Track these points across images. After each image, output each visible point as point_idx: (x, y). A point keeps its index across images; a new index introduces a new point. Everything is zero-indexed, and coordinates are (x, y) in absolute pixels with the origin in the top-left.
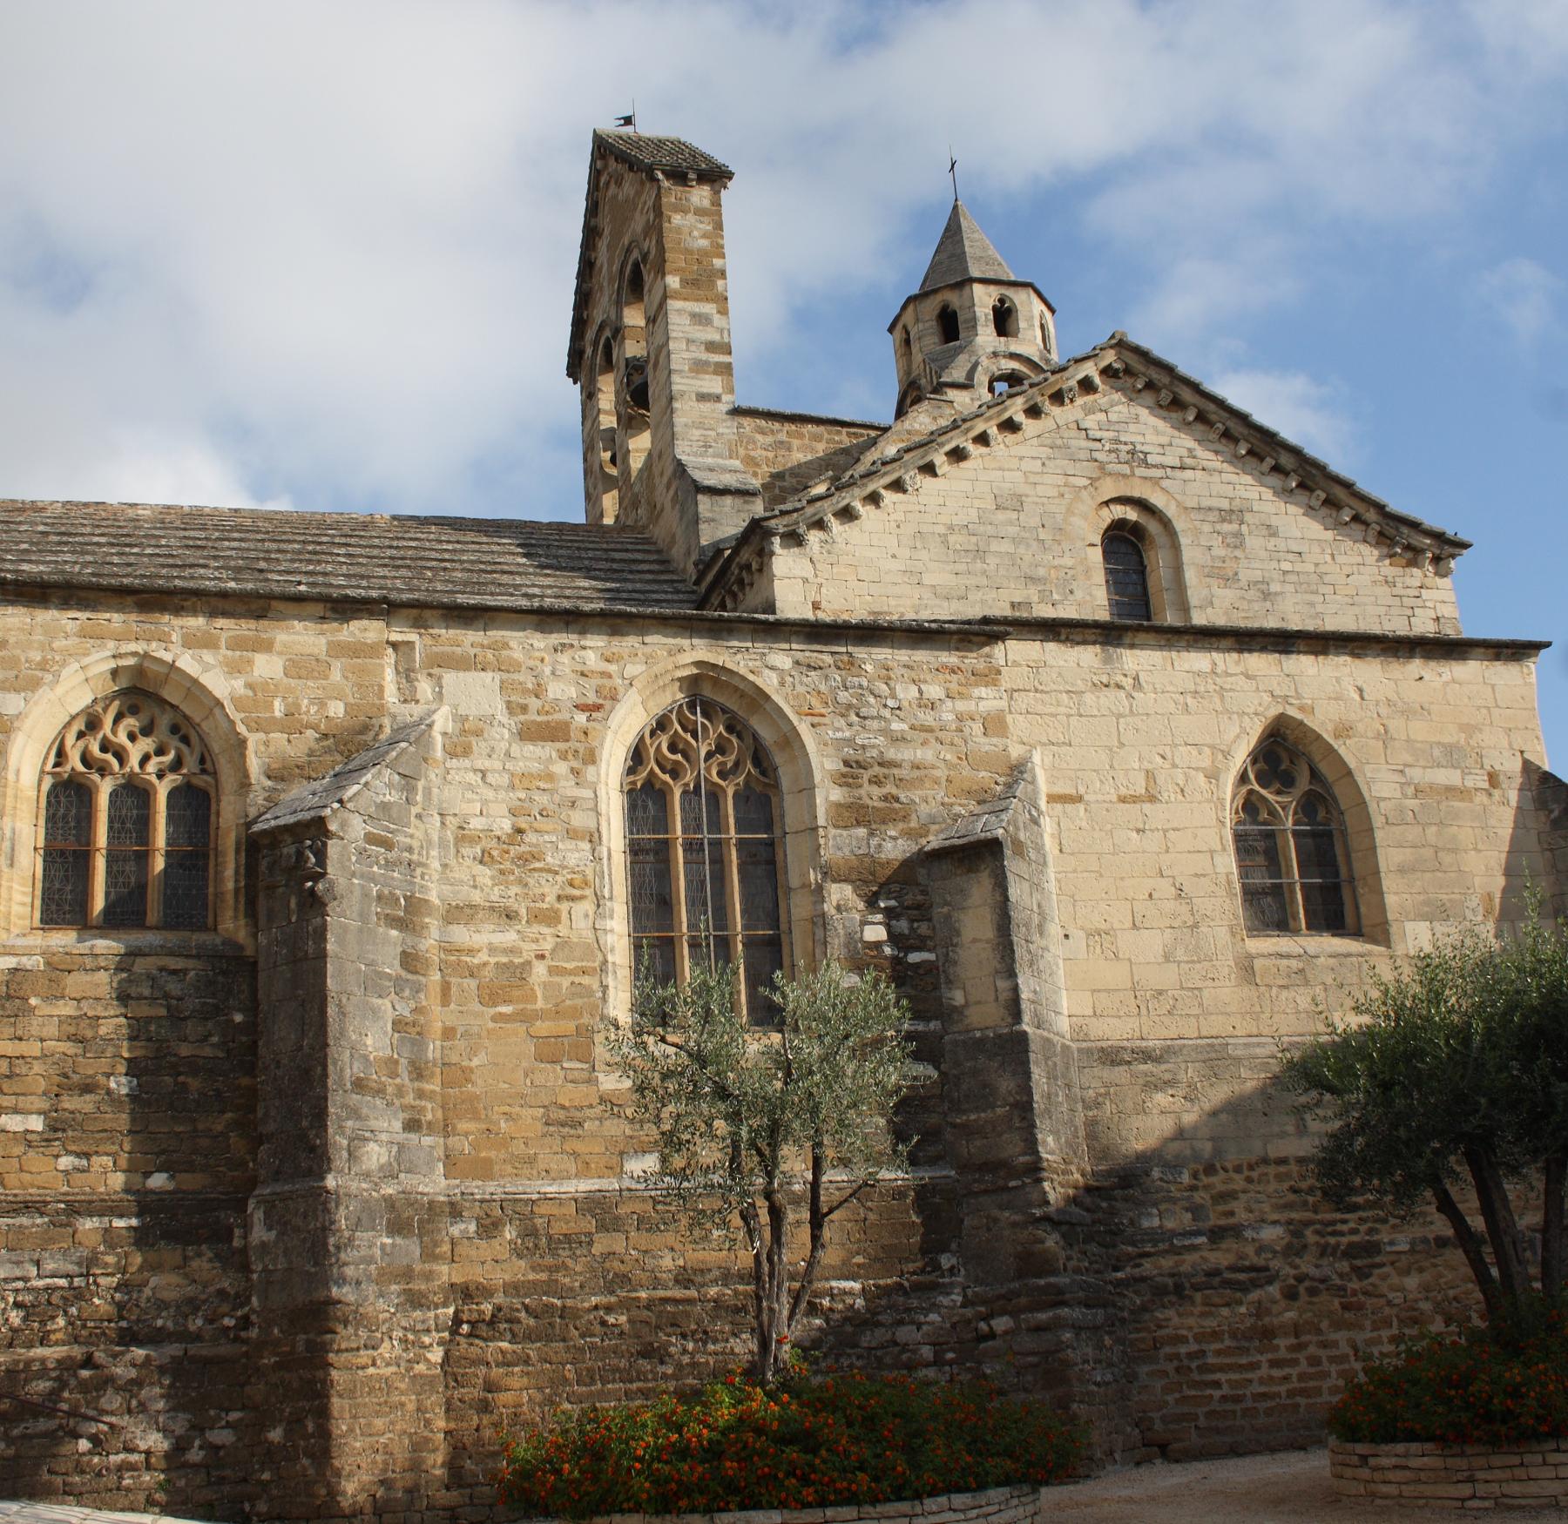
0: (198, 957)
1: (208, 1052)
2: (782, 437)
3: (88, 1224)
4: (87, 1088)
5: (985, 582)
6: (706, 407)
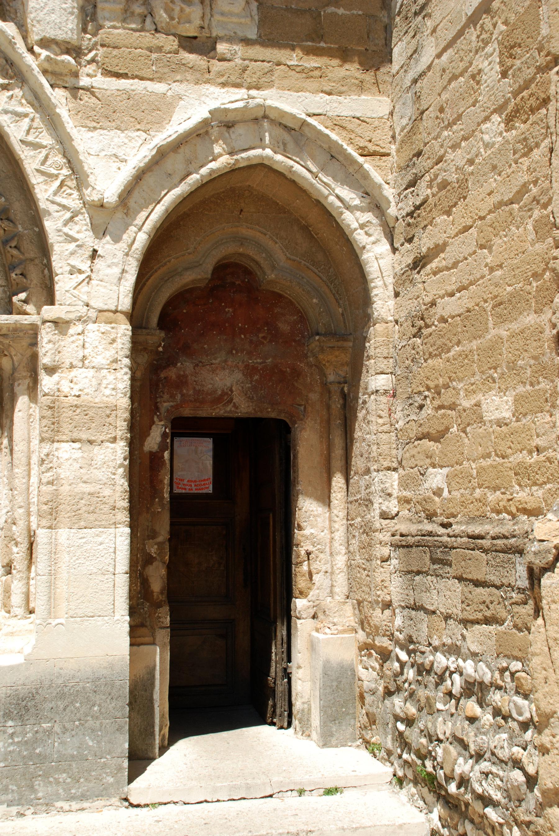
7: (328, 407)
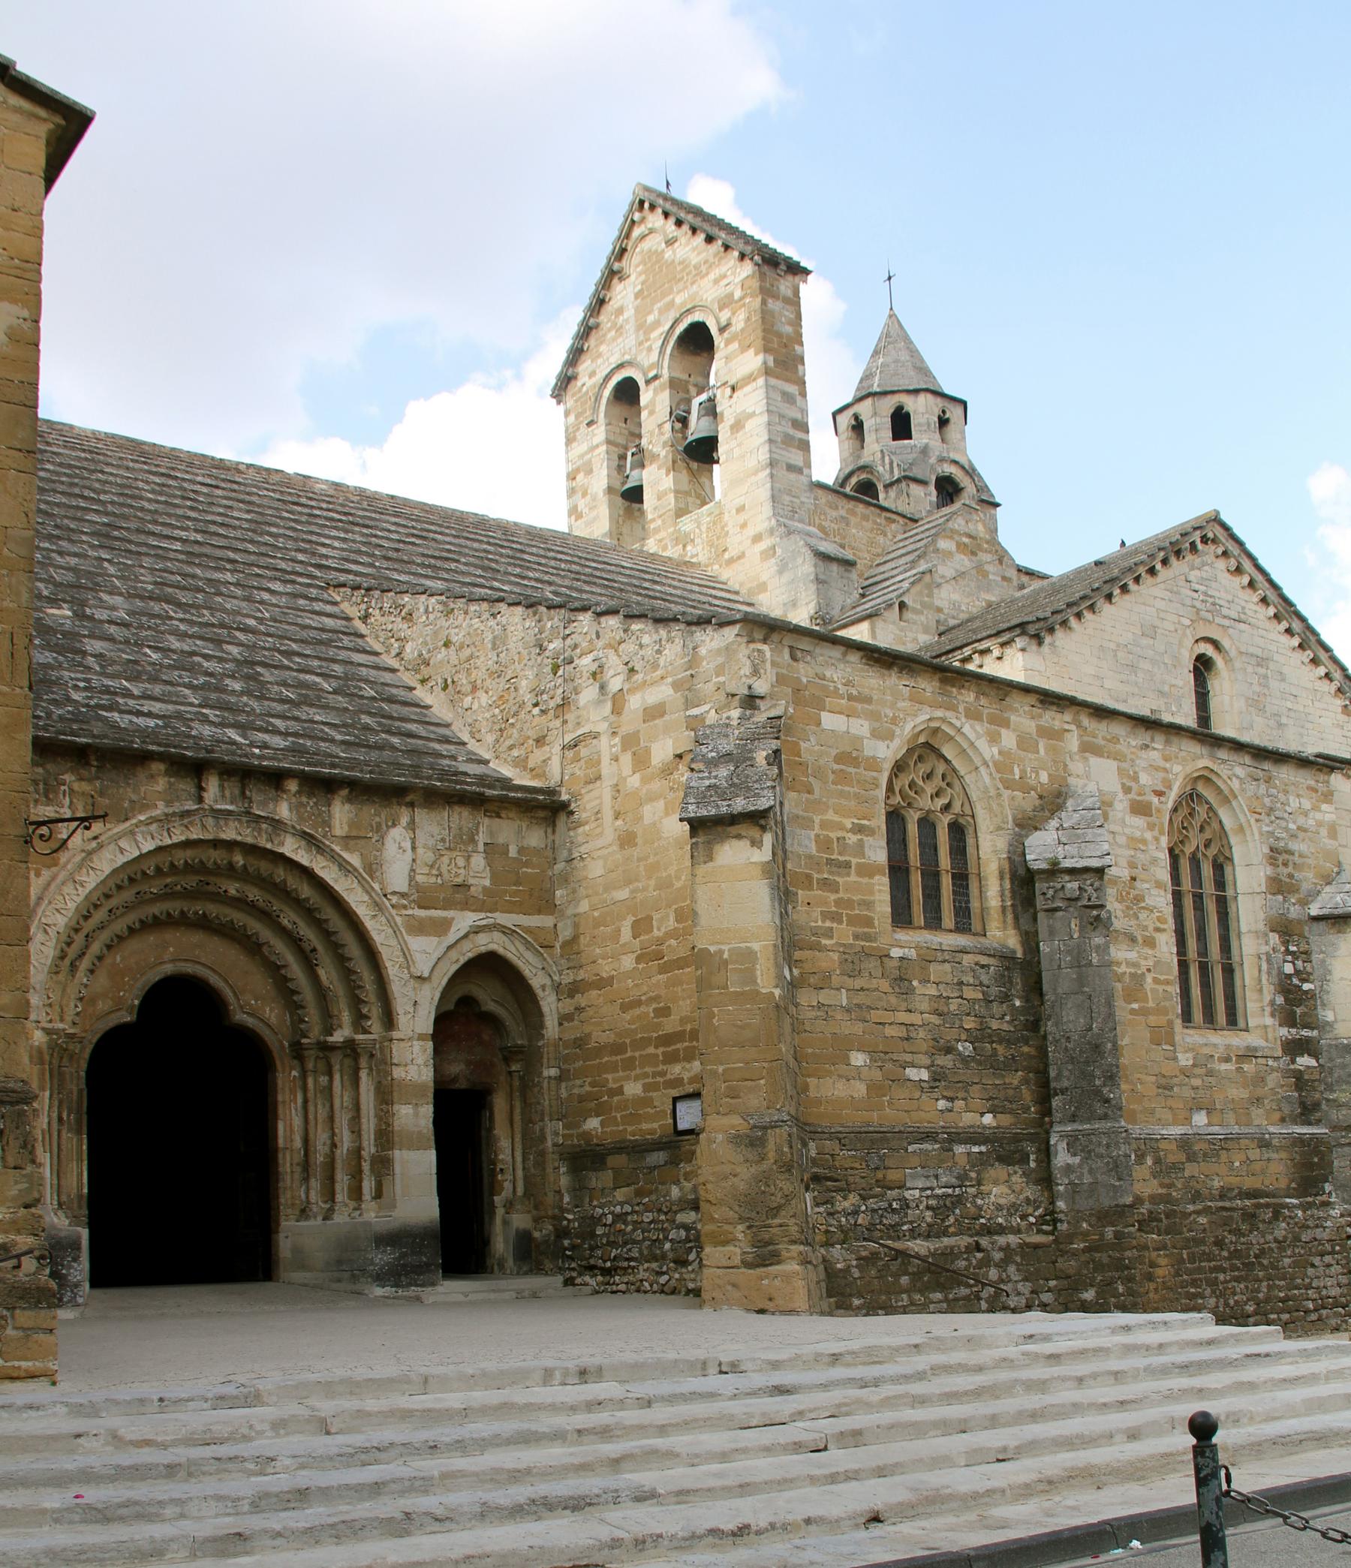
0: (994, 956)
1: (1005, 1027)
2: (843, 513)
3: (960, 1149)
4: (949, 1050)
5: (1136, 690)
6: (793, 476)
7: (511, 1086)
